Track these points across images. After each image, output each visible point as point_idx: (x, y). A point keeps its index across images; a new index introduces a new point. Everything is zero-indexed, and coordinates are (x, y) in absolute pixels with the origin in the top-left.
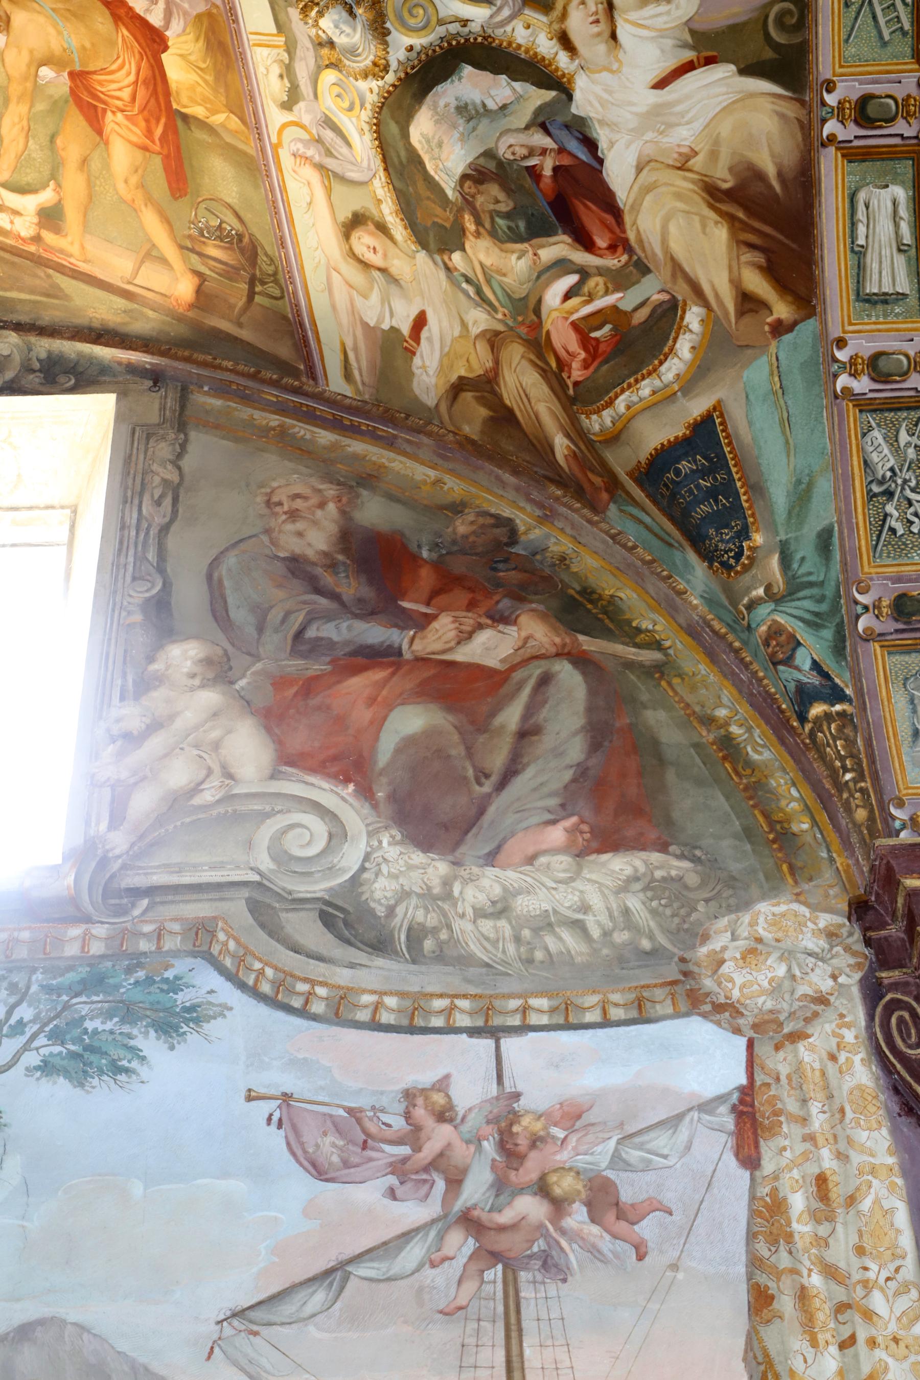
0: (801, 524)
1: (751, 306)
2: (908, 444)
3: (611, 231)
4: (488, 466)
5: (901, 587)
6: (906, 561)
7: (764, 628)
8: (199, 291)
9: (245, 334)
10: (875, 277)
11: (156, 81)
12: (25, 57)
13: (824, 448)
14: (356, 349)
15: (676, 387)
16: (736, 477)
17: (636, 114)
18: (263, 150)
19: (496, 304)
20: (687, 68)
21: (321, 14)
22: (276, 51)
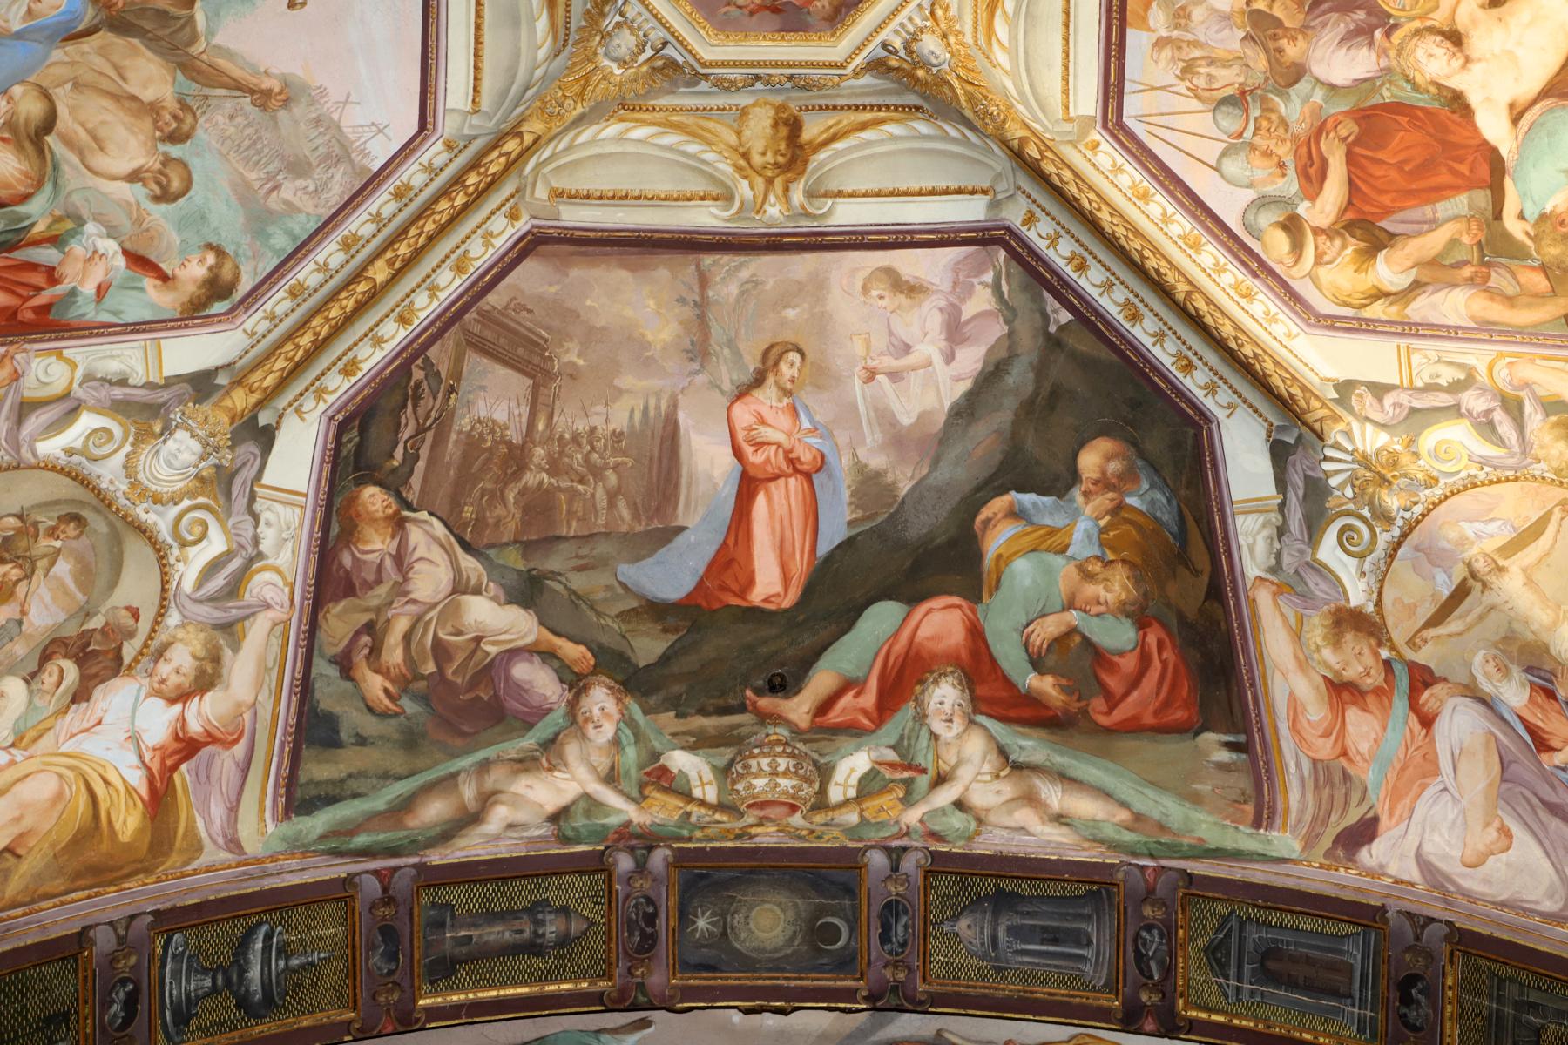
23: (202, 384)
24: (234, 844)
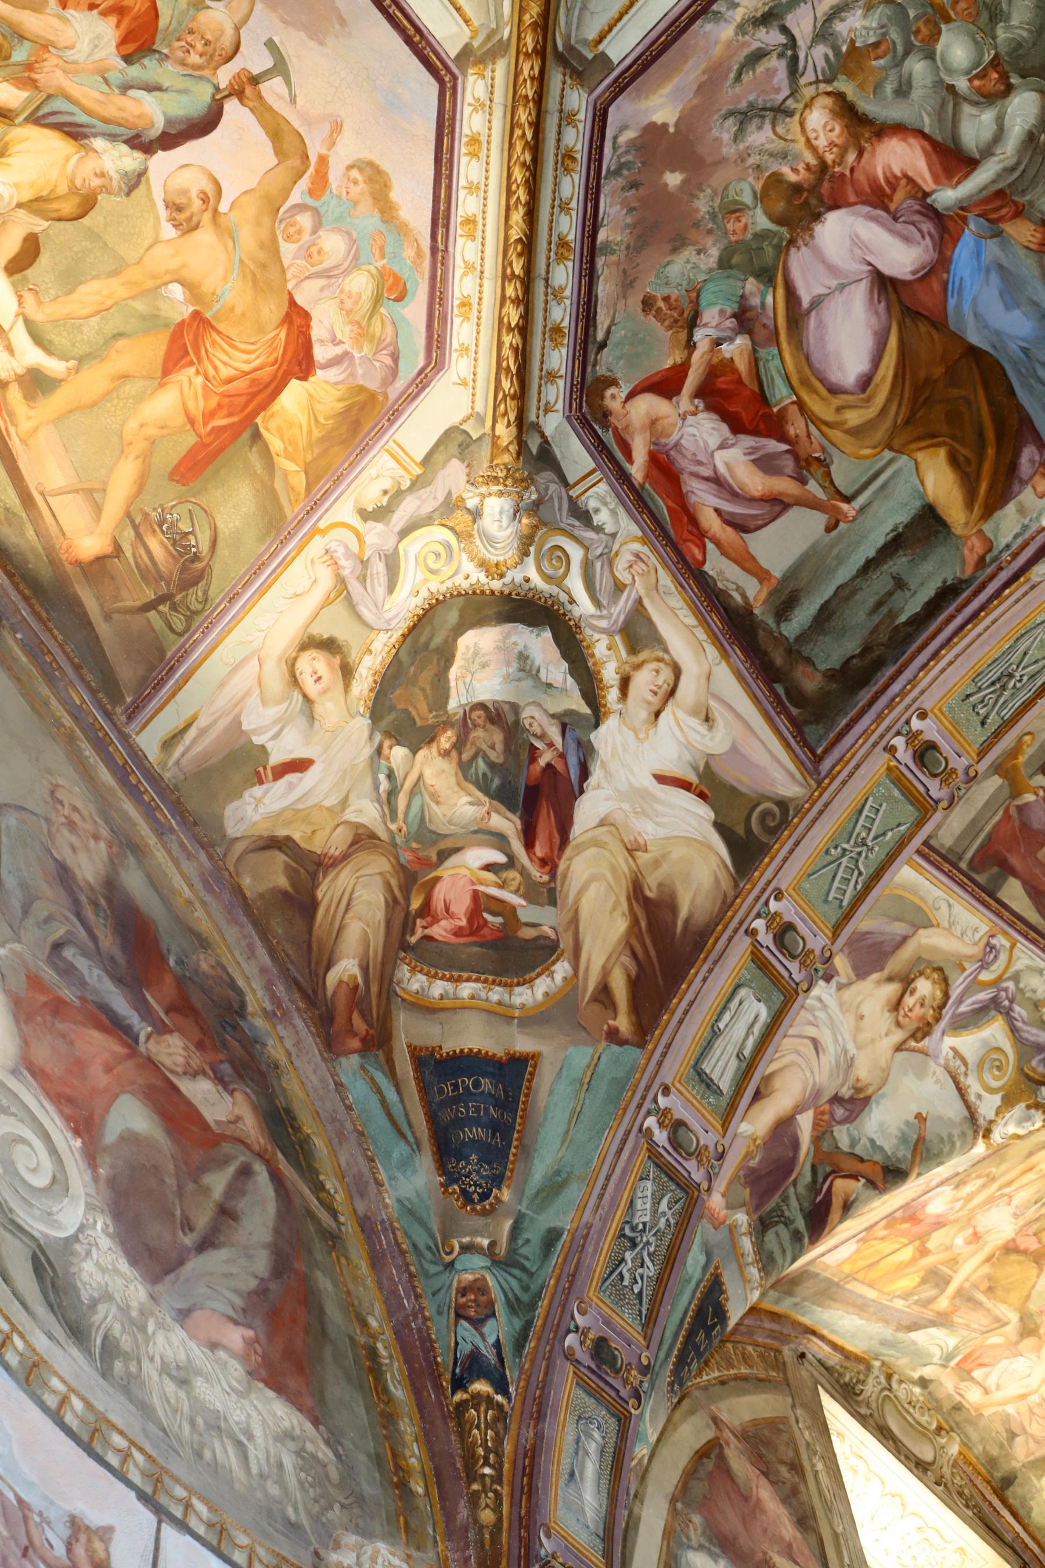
0: (540, 1209)
1: (605, 1000)
2: (664, 1214)
3: (551, 849)
4: (250, 929)
5: (609, 1333)
6: (618, 1310)
7: (469, 1277)
8: (100, 560)
9: (103, 629)
10: (713, 1061)
11: (267, 391)
12: (175, 263)
13: (591, 1161)
14: (203, 732)
15: (517, 1013)
16: (518, 1128)
17: (630, 783)
18: (301, 523)
19: (401, 815)
20: (685, 785)
21: (501, 494)
22: (404, 473)
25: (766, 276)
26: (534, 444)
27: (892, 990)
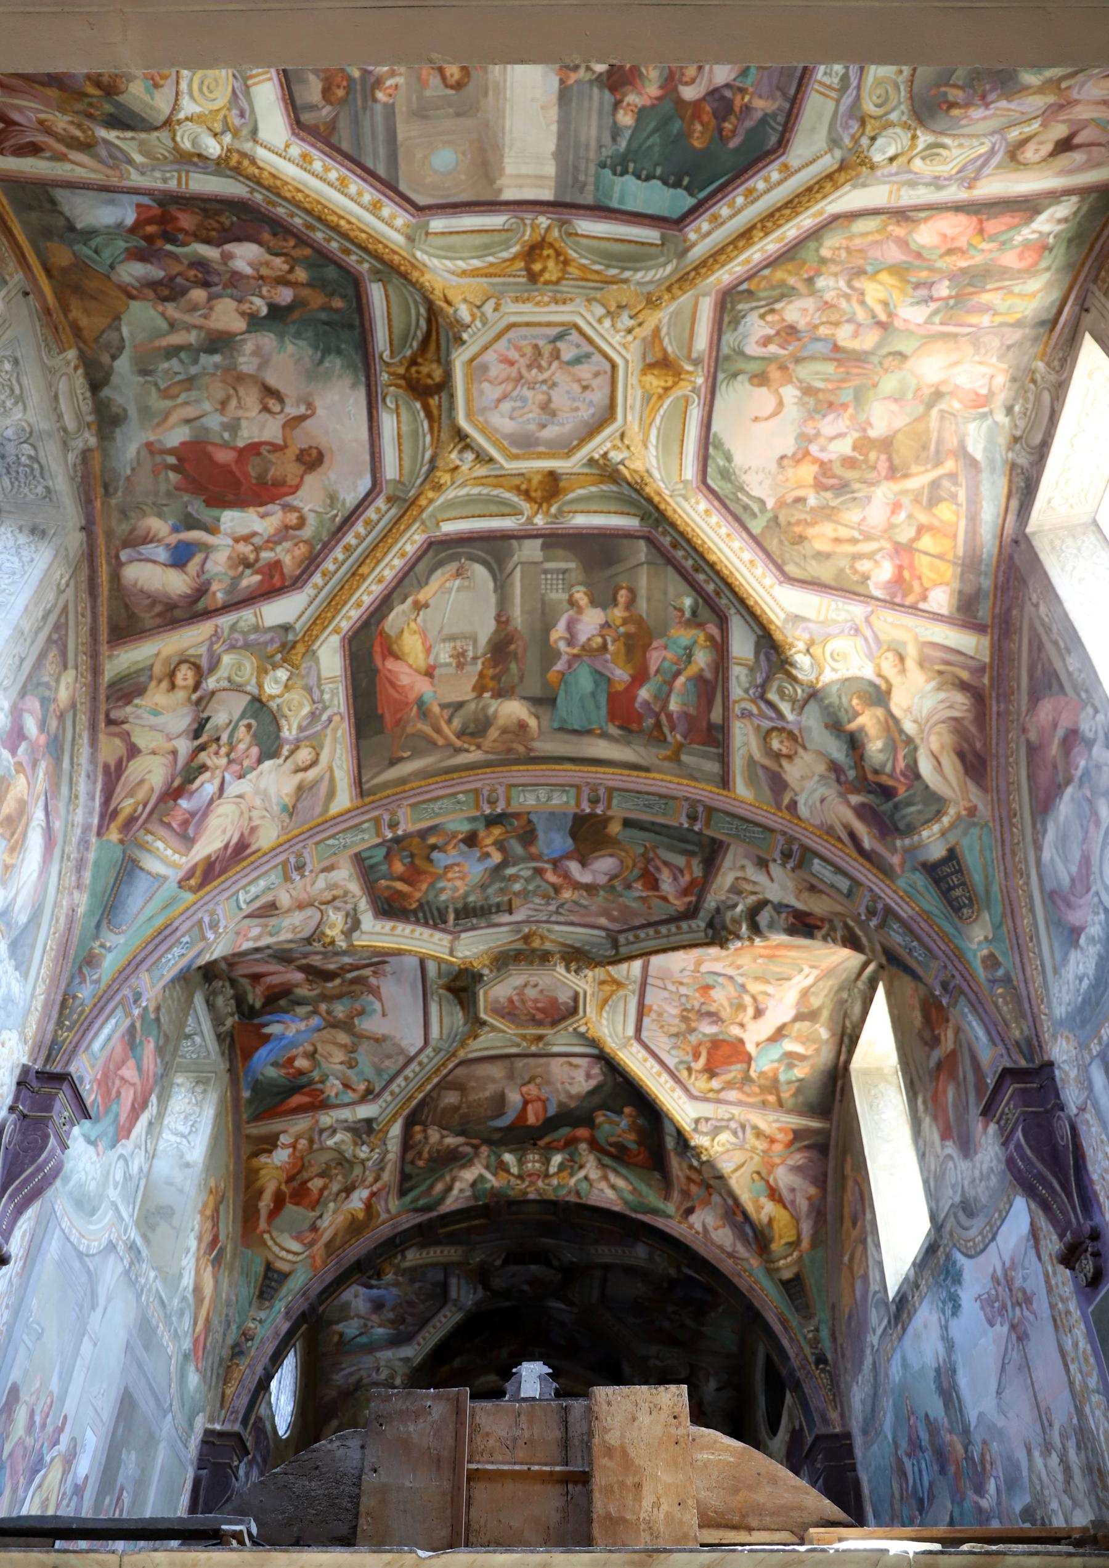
23: (369, 1121)
24: (388, 1211)
25: (613, 888)
26: (710, 932)
27: (785, 763)
